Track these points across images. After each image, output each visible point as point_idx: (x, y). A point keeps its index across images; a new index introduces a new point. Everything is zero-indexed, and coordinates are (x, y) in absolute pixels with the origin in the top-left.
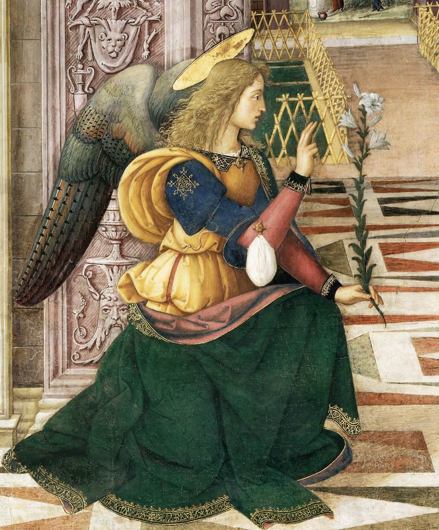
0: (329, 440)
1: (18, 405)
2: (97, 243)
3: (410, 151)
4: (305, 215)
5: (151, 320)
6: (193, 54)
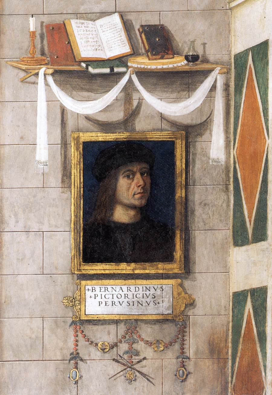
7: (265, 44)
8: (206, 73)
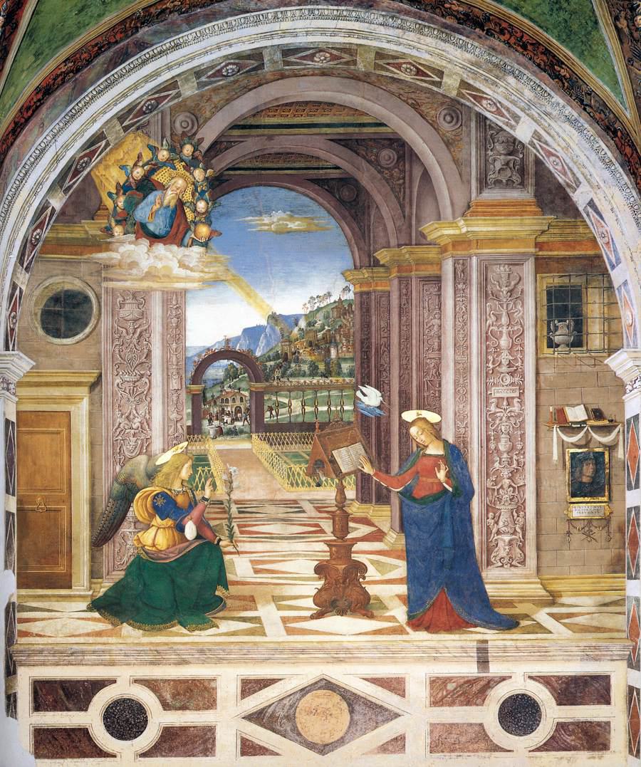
1: (93, 586)
2: (125, 523)
3: (249, 489)
4: (208, 513)
6: (164, 451)
7: (638, 415)
8: (616, 426)
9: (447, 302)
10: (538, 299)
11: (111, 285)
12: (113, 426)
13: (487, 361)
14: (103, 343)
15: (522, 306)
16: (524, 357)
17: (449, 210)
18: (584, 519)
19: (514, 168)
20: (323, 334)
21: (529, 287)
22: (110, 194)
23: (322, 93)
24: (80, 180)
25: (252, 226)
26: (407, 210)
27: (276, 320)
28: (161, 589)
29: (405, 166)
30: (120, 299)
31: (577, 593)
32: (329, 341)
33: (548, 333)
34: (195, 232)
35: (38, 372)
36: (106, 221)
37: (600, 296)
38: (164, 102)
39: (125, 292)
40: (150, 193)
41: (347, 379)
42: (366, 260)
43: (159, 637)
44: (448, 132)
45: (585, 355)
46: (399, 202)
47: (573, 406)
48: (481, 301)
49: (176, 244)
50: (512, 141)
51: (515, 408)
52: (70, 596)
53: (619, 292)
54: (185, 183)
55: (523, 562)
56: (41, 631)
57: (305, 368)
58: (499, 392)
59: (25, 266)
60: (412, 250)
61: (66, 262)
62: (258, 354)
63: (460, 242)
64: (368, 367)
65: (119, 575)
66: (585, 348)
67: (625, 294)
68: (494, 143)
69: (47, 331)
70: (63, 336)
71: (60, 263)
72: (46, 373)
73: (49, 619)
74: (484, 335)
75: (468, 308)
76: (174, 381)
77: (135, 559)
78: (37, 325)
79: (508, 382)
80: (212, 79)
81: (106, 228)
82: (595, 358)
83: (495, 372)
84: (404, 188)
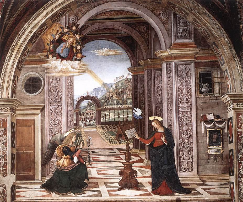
0: (85, 184)
1: (42, 179)
4: (81, 153)
5: (61, 168)
6: (66, 132)
8: (224, 121)
9: (164, 78)
10: (196, 77)
11: (48, 74)
12: (49, 124)
13: (179, 99)
14: (45, 95)
15: (190, 79)
16: (191, 97)
17: (164, 47)
18: (214, 154)
19: (187, 32)
20: (121, 90)
21: (193, 73)
22: (48, 44)
23: (120, 7)
24: (38, 39)
25: (96, 54)
26: (150, 47)
27: (105, 86)
28: (65, 180)
29: (149, 32)
30: (51, 79)
31: (212, 181)
32: (123, 92)
33: (200, 88)
34: (76, 56)
35: (24, 106)
36: (47, 53)
37: (218, 74)
38: (66, 12)
39: (53, 77)
40: (62, 43)
41: (130, 106)
42: (135, 63)
43: (65, 197)
44: (164, 19)
45: (213, 96)
46: (147, 44)
47: (209, 114)
48: (176, 77)
49: (70, 60)
50: (186, 22)
51: (189, 115)
52: (34, 183)
53: (225, 73)
54: (73, 40)
55: (192, 170)
56: (25, 195)
57: (115, 102)
58: (183, 109)
59: (19, 69)
60: (152, 60)
61: (33, 67)
62: (98, 97)
63: (169, 57)
64: (137, 101)
65: (51, 176)
66: (213, 94)
67: (227, 74)
68: (180, 23)
69: (27, 91)
70: (32, 93)
71: (31, 68)
72: (26, 105)
73: (28, 191)
74: (177, 89)
75: (171, 80)
76: (70, 108)
77: (56, 170)
78: (23, 89)
79: (186, 106)
80: (82, 4)
81: (46, 55)
82: (216, 97)
83: (181, 103)
84: (149, 39)
